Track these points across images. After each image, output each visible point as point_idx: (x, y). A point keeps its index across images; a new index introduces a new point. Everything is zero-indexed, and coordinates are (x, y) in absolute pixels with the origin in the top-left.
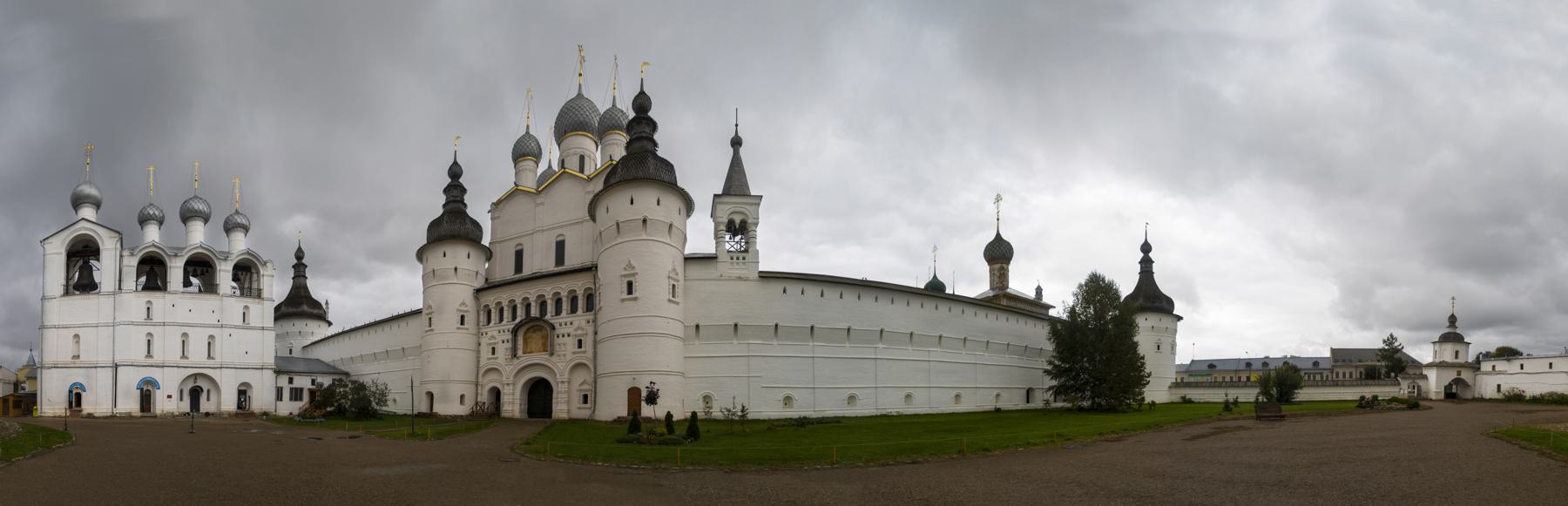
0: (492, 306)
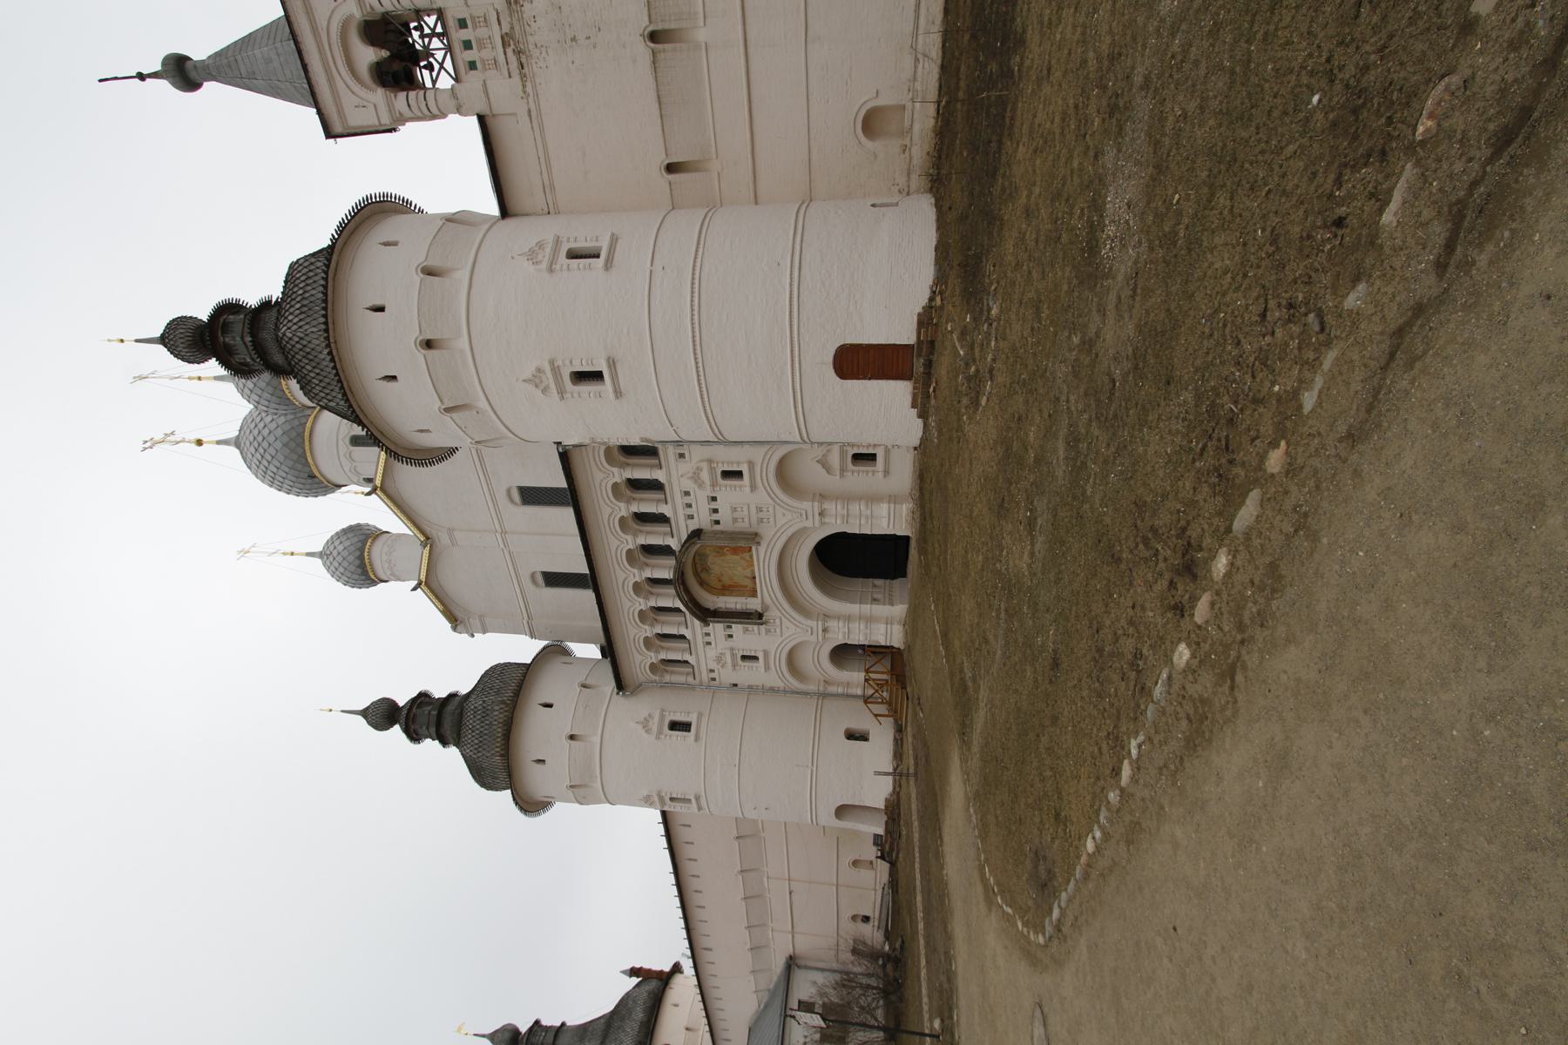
0: (653, 657)
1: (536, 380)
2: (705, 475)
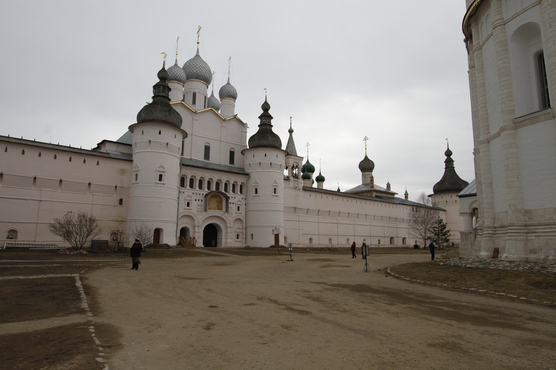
1: (276, 182)
2: (239, 203)
